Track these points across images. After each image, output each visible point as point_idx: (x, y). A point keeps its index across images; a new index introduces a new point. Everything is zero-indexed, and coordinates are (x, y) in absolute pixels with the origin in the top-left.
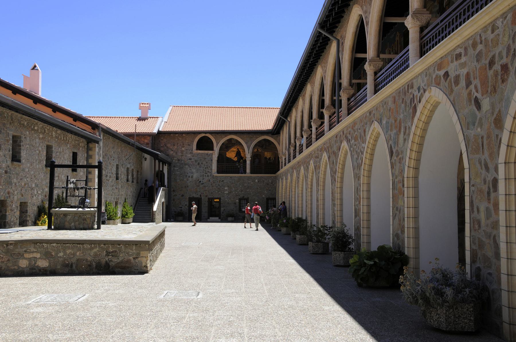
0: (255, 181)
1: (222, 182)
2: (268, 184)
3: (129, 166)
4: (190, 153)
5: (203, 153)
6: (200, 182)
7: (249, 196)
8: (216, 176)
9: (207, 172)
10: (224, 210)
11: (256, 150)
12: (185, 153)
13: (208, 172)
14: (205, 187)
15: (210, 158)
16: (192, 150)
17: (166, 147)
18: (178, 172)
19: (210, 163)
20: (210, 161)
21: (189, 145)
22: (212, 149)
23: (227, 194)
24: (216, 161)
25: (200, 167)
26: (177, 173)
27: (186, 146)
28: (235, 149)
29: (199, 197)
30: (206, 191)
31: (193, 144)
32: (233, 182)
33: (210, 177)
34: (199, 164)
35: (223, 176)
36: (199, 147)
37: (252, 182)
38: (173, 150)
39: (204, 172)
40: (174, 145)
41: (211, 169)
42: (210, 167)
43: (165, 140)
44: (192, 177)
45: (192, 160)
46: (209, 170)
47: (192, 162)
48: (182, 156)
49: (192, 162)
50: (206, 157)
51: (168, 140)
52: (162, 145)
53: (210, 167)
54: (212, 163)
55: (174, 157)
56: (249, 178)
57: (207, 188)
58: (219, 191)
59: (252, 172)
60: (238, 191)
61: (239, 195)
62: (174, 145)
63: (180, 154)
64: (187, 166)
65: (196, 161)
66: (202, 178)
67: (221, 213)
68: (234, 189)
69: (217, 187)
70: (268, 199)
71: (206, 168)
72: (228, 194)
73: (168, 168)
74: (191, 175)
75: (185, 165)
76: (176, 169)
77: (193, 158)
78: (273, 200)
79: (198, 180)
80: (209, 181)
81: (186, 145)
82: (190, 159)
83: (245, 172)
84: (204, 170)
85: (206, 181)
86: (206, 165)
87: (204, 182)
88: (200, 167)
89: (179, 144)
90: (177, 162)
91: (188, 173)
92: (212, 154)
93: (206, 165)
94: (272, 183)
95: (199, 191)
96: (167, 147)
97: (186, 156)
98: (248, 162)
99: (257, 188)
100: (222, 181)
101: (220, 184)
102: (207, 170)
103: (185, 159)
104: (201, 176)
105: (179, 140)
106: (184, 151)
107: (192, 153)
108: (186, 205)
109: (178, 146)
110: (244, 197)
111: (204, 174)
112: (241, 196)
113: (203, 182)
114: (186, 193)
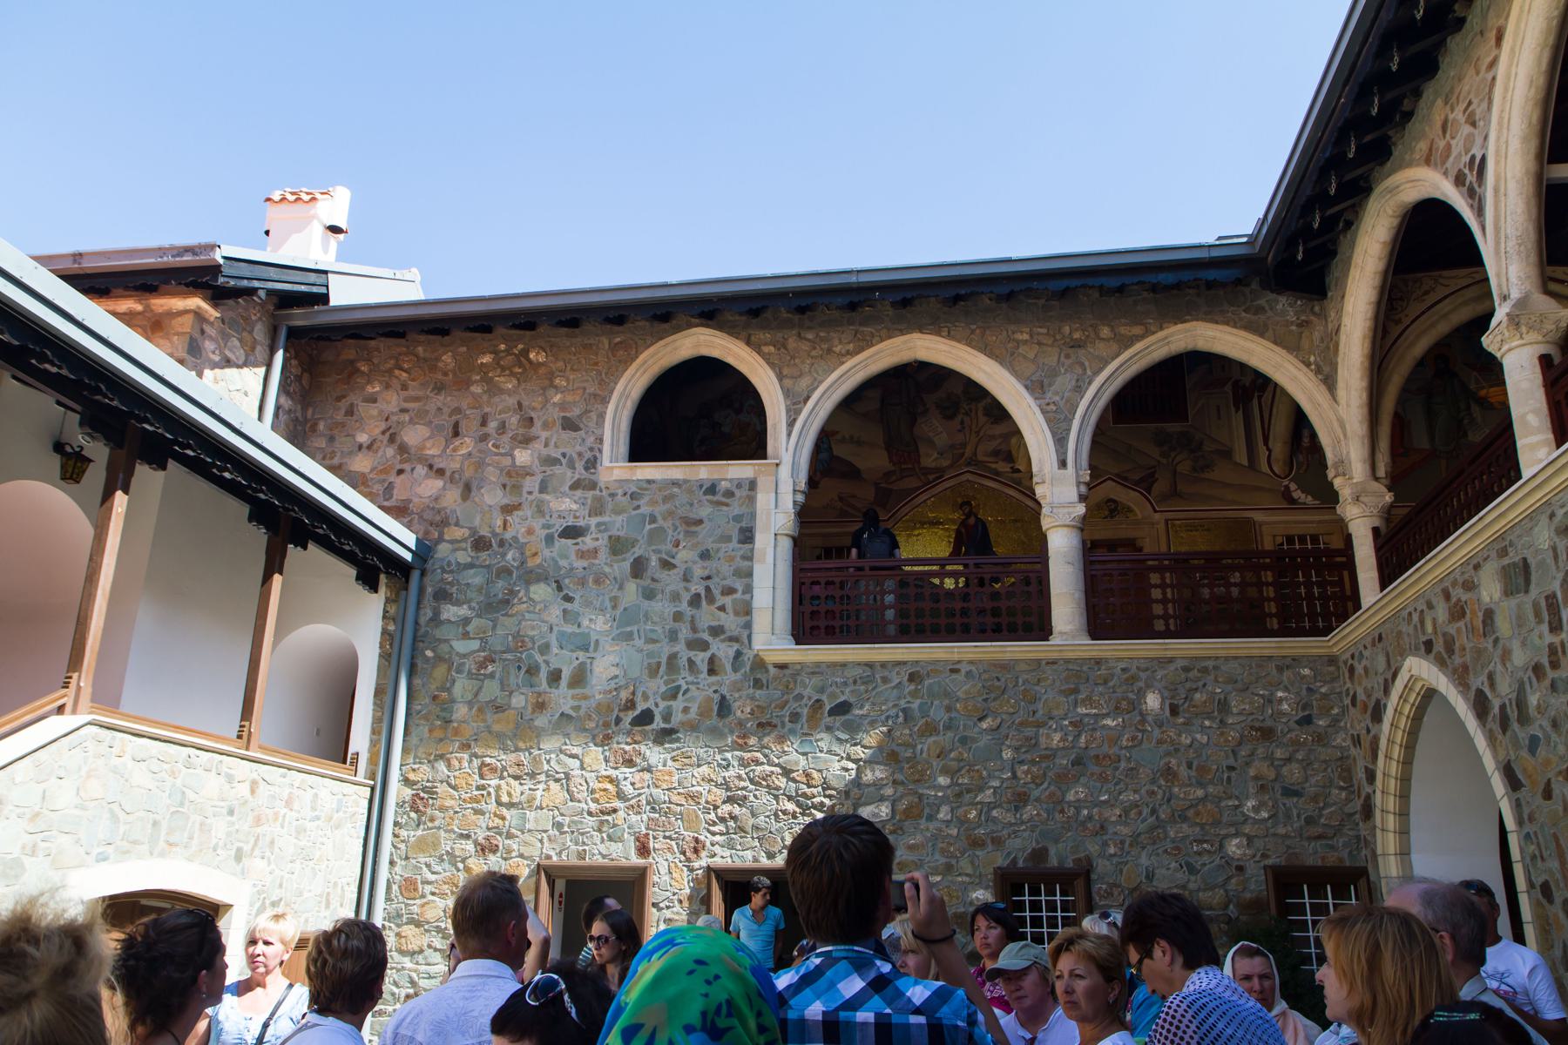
0: (1135, 705)
2: (1267, 734)
4: (575, 486)
5: (675, 483)
7: (1093, 848)
8: (782, 667)
9: (706, 636)
12: (531, 484)
13: (716, 631)
15: (738, 518)
16: (592, 464)
17: (390, 452)
18: (466, 636)
19: (732, 559)
20: (734, 544)
21: (570, 425)
22: (753, 445)
24: (786, 545)
25: (649, 595)
26: (460, 646)
27: (544, 435)
29: (635, 860)
31: (602, 416)
32: (938, 714)
33: (729, 677)
34: (638, 568)
35: (844, 665)
36: (643, 446)
37: (1116, 711)
38: (440, 472)
39: (685, 632)
40: (456, 434)
41: (746, 610)
42: (729, 591)
43: (391, 401)
44: (579, 679)
45: (588, 542)
46: (730, 622)
47: (582, 555)
48: (508, 509)
49: (582, 555)
50: (705, 511)
51: (417, 399)
52: (363, 438)
54: (749, 558)
55: (444, 523)
56: (1077, 675)
59: (1099, 624)
60: (987, 796)
61: (997, 842)
62: (456, 434)
64: (541, 591)
65: (618, 546)
66: (658, 685)
68: (943, 780)
71: (695, 601)
73: (392, 610)
74: (565, 660)
75: (532, 577)
76: (450, 612)
77: (594, 521)
78: (1341, 893)
79: (631, 705)
81: (546, 426)
82: (572, 532)
83: (1041, 629)
84: (678, 617)
85: (693, 714)
86: (698, 572)
87: (678, 717)
88: (649, 595)
89: (493, 425)
90: (463, 557)
91: (545, 649)
92: (753, 485)
93: (698, 572)
94: (1306, 721)
96: (403, 449)
97: (540, 510)
98: (1062, 544)
99: (1169, 773)
100: (832, 712)
102: (707, 616)
103: (530, 532)
104: (653, 671)
105: (493, 390)
106: (527, 472)
107: (593, 485)
109: (484, 438)
110: (1039, 854)
111: (680, 647)
112: (1019, 847)
113: (667, 717)
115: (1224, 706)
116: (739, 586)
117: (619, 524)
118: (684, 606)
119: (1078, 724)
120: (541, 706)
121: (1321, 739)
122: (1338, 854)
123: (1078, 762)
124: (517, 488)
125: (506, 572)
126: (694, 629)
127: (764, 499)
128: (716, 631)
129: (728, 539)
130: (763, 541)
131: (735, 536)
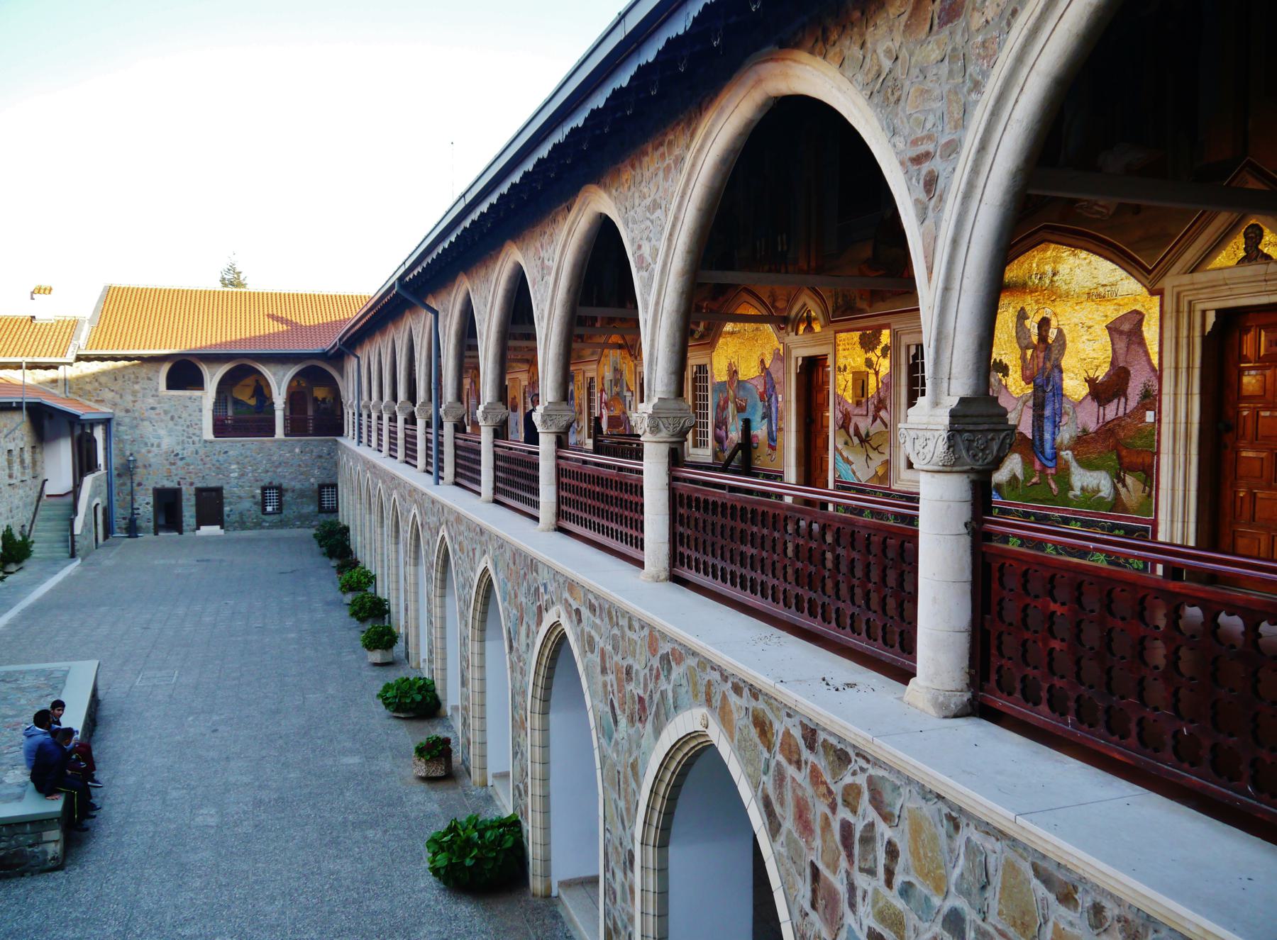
1: (225, 455)
2: (320, 457)
3: (11, 447)
4: (153, 396)
6: (177, 455)
10: (231, 511)
11: (295, 383)
12: (140, 395)
13: (194, 434)
14: (188, 465)
21: (149, 379)
23: (236, 478)
28: (250, 381)
29: (177, 486)
30: (190, 473)
32: (249, 453)
33: (197, 445)
34: (172, 418)
37: (289, 452)
38: (113, 391)
39: (186, 434)
40: (116, 380)
41: (201, 429)
42: (196, 424)
44: (159, 446)
45: (157, 411)
46: (197, 432)
47: (157, 414)
48: (134, 402)
49: (157, 414)
50: (189, 403)
53: (196, 424)
54: (201, 416)
57: (192, 467)
58: (218, 474)
60: (260, 471)
61: (262, 480)
63: (129, 398)
64: (146, 423)
66: (180, 447)
67: (225, 517)
69: (213, 465)
70: (321, 487)
71: (188, 426)
72: (238, 478)
74: (156, 441)
76: (122, 428)
78: (332, 488)
79: (173, 452)
80: (197, 453)
81: (143, 379)
82: (153, 408)
83: (271, 432)
89: (126, 377)
92: (201, 397)
94: (329, 454)
95: (176, 475)
96: (100, 384)
101: (220, 458)
102: (191, 430)
104: (178, 444)
107: (157, 396)
108: (148, 504)
109: (124, 381)
110: (271, 483)
111: (184, 438)
112: (266, 482)
114: (147, 479)
115: (312, 451)
116: (199, 423)
117: (166, 407)
118: (185, 428)
119: (280, 456)
120: (149, 452)
121: (331, 458)
122: (333, 480)
123: (280, 464)
124: (135, 396)
125: (136, 418)
126: (188, 433)
127: (204, 401)
128: (194, 434)
129: (195, 411)
130: (204, 411)
131: (197, 410)
